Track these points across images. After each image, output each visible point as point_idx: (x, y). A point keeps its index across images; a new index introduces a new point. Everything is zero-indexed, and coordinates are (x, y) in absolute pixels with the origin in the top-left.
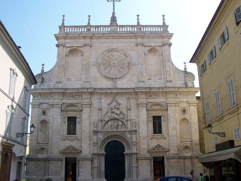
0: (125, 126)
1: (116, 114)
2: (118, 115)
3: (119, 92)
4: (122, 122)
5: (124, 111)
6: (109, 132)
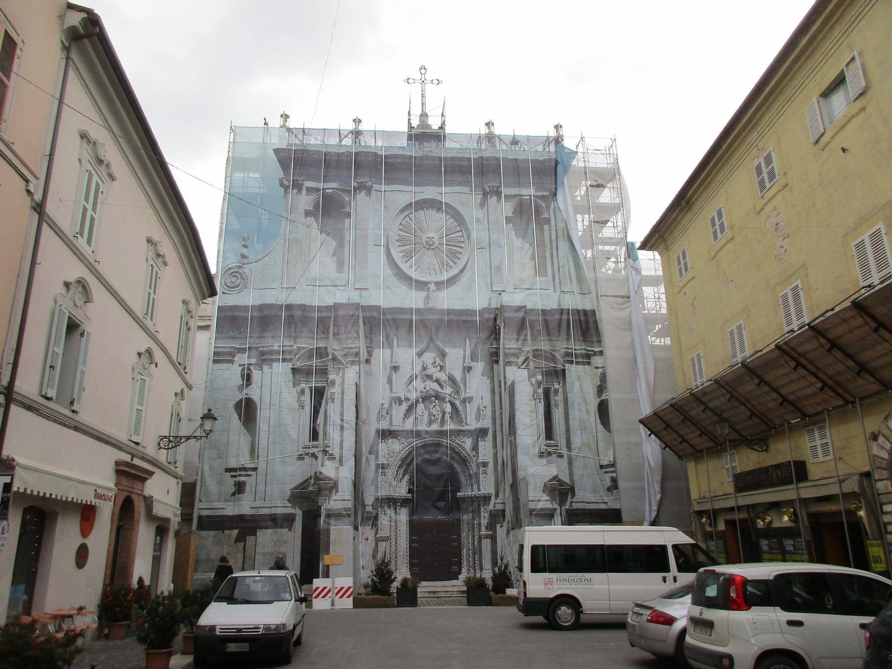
1: (437, 381)
2: (441, 386)
4: (453, 405)
5: (458, 374)
6: (418, 434)
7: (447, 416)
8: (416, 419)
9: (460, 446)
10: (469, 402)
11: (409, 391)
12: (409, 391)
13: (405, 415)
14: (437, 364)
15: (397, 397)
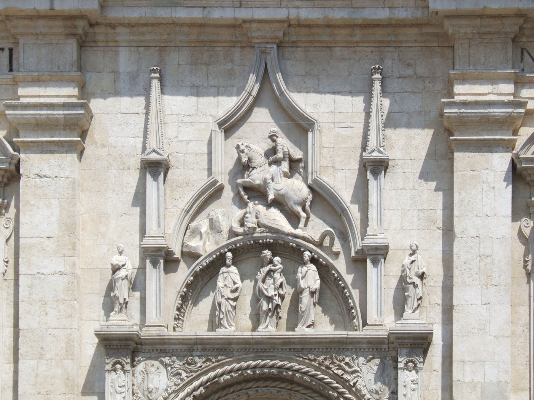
0: (345, 299)
3: (301, 25)
7: (306, 299)
8: (216, 307)
9: (344, 382)
10: (375, 263)
11: (197, 232)
12: (197, 232)
13: (184, 298)
14: (280, 155)
15: (159, 249)
